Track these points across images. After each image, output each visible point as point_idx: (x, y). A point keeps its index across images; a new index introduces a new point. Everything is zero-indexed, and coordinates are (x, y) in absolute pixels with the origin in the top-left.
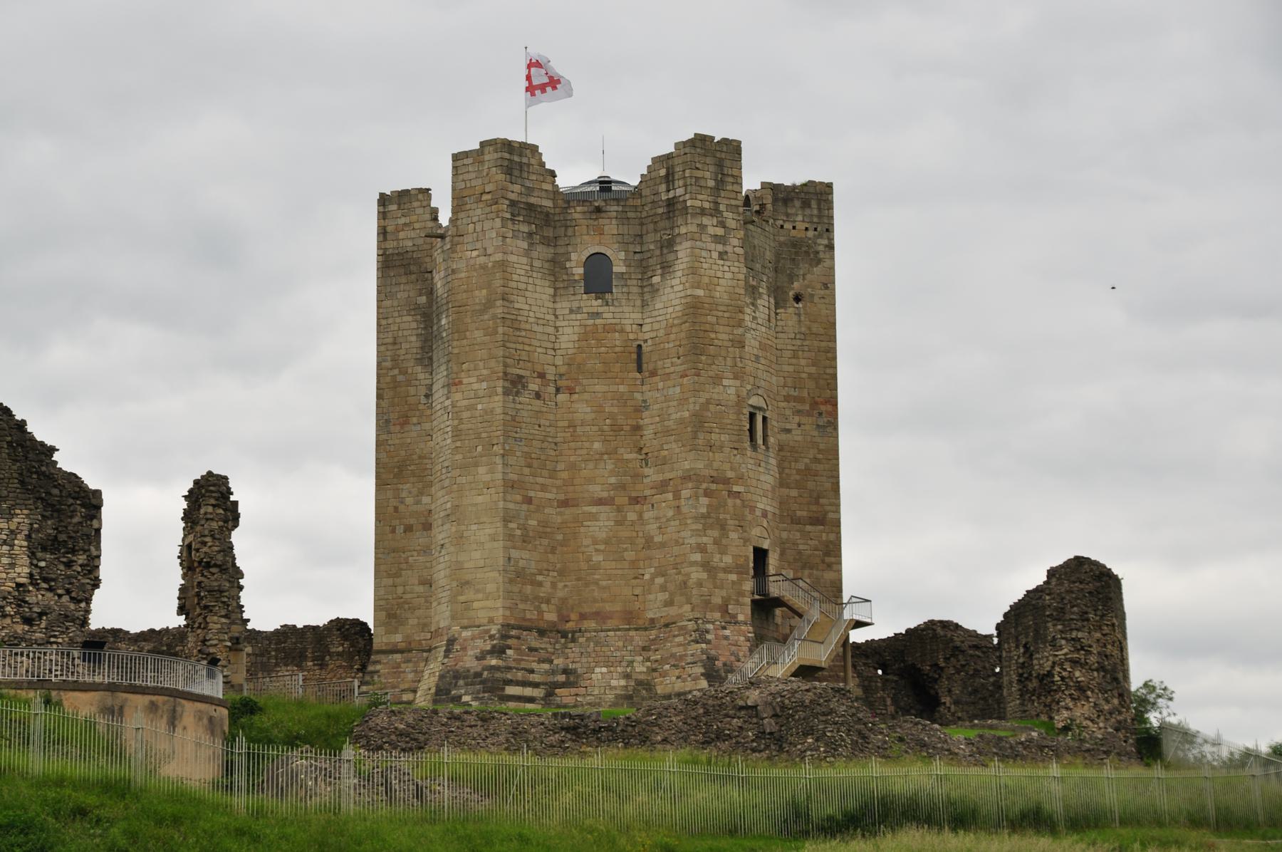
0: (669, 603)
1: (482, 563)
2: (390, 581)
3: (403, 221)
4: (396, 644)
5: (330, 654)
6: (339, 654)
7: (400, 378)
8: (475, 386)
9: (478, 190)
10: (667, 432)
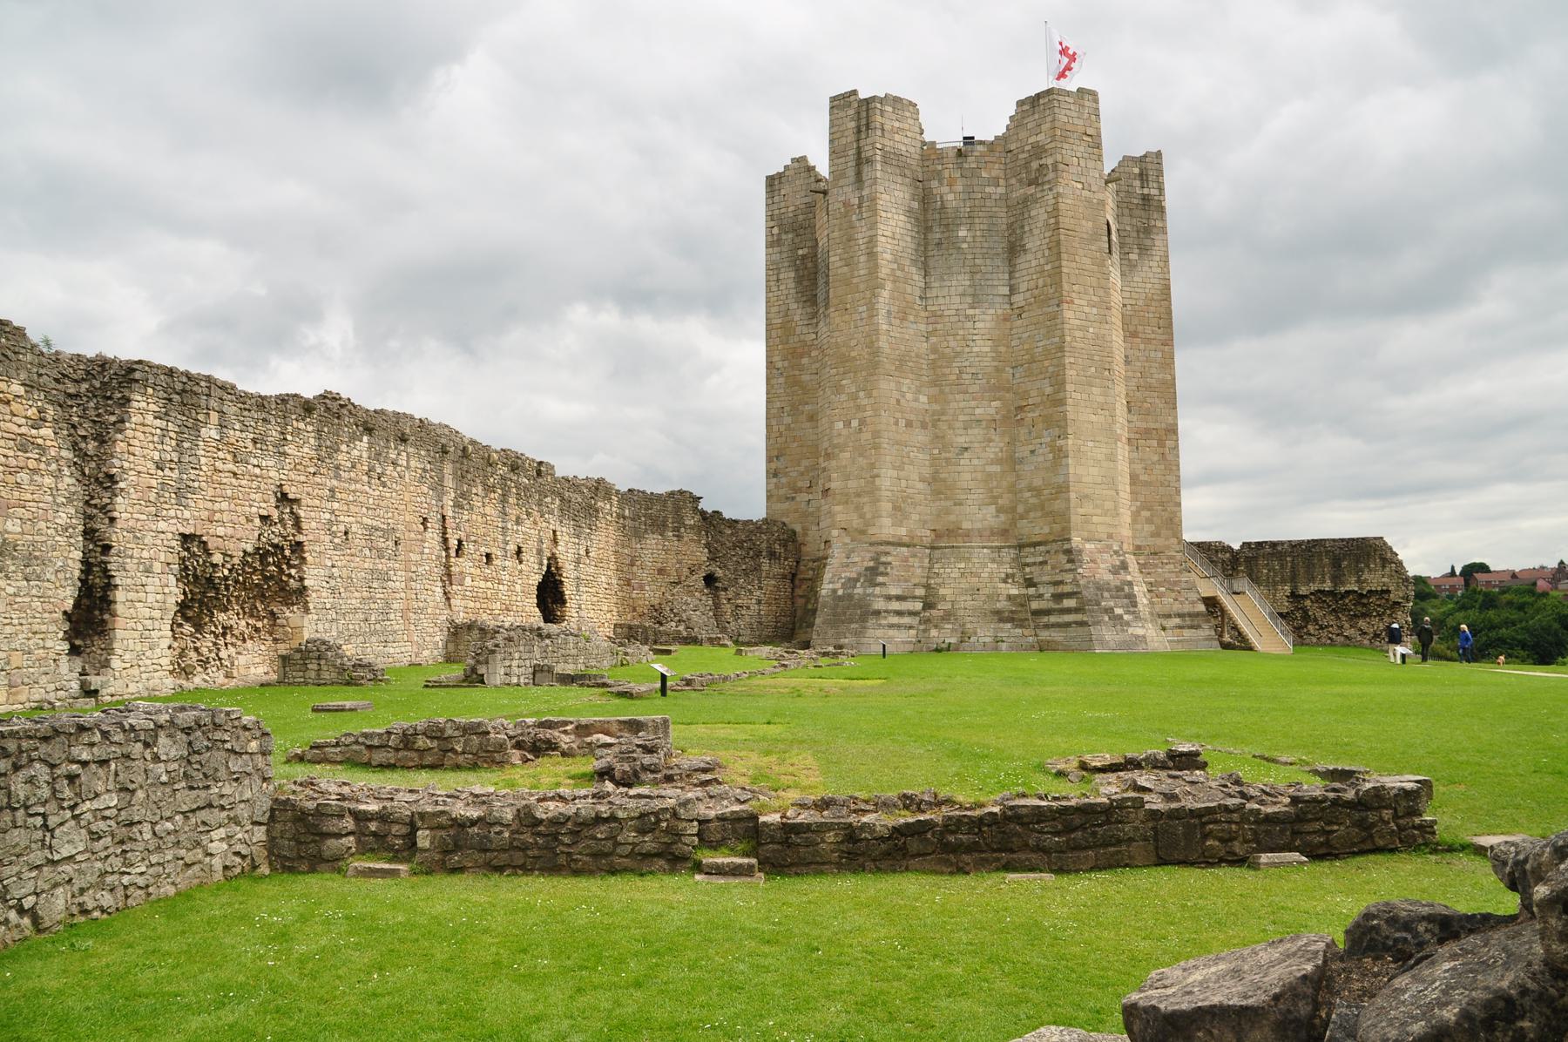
0: (1156, 534)
1: (1099, 480)
2: (895, 473)
3: (897, 124)
4: (900, 537)
5: (685, 526)
6: (692, 527)
7: (899, 273)
8: (1087, 309)
9: (1081, 130)
10: (1150, 388)
